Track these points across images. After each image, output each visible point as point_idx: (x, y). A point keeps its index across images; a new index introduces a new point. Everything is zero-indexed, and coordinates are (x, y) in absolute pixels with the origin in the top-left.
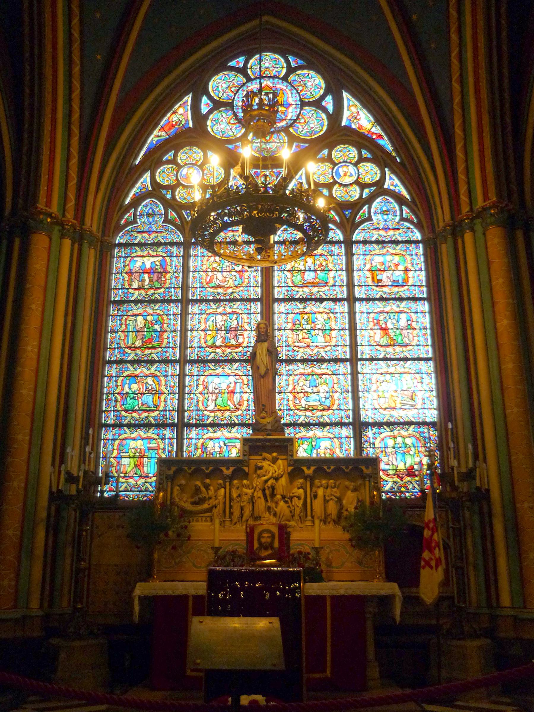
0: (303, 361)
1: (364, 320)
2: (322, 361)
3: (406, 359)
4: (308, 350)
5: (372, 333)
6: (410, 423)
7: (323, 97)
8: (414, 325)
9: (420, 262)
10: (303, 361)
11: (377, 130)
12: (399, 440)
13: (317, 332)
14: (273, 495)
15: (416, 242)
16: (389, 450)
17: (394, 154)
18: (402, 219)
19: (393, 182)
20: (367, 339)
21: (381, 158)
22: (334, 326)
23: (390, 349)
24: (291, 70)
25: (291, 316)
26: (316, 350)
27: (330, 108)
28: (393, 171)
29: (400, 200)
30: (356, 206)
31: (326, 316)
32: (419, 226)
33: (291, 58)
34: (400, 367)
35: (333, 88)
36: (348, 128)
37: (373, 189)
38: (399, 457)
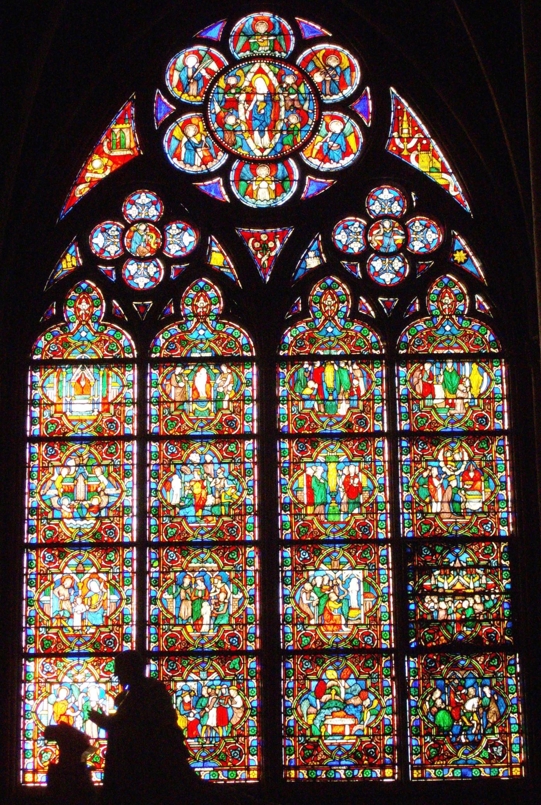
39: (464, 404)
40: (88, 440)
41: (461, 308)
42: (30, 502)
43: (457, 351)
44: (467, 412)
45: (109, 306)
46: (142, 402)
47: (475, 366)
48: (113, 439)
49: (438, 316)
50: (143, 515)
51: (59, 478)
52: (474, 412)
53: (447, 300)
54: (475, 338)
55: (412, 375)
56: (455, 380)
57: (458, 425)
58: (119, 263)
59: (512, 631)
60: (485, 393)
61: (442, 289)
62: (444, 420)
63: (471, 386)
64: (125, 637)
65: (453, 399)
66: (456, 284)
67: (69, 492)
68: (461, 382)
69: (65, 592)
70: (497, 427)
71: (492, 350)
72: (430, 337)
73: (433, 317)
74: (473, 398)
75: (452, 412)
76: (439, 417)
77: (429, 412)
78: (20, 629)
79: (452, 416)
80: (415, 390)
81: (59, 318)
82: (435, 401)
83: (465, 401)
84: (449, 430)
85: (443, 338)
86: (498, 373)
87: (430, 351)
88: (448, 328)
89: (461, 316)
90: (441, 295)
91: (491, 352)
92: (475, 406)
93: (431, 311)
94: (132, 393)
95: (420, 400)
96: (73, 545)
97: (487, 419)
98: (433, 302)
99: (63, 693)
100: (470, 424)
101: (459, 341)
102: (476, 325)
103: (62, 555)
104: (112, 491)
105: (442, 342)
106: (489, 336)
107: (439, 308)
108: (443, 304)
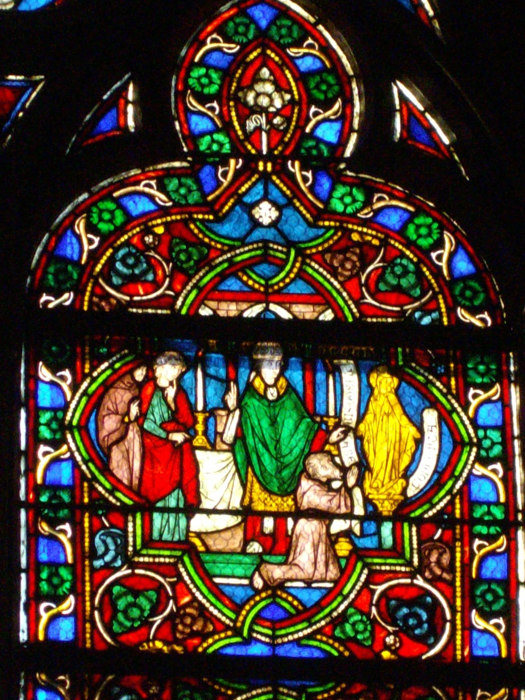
39: (332, 540)
41: (329, 133)
43: (305, 311)
44: (345, 574)
47: (384, 383)
49: (224, 160)
52: (375, 577)
53: (266, 94)
54: (389, 262)
55: (96, 403)
56: (292, 435)
57: (301, 630)
60: (427, 495)
61: (245, 48)
62: (237, 608)
63: (363, 465)
65: (279, 517)
66: (306, 31)
68: (318, 442)
70: (483, 647)
71: (462, 314)
72: (184, 248)
73: (200, 159)
74: (373, 516)
75: (278, 573)
76: (217, 591)
77: (170, 570)
79: (276, 588)
80: (105, 469)
82: (200, 523)
83: (338, 526)
84: (256, 650)
85: (243, 255)
86: (490, 415)
87: (183, 305)
88: (266, 213)
89: (326, 163)
90: (236, 75)
91: (458, 324)
92: (380, 551)
93: (193, 138)
95: (125, 511)
97: (434, 608)
98: (203, 99)
100: (355, 627)
101: (314, 269)
102: (391, 207)
105: (234, 270)
106: (450, 256)
107: (227, 128)
108: (246, 111)
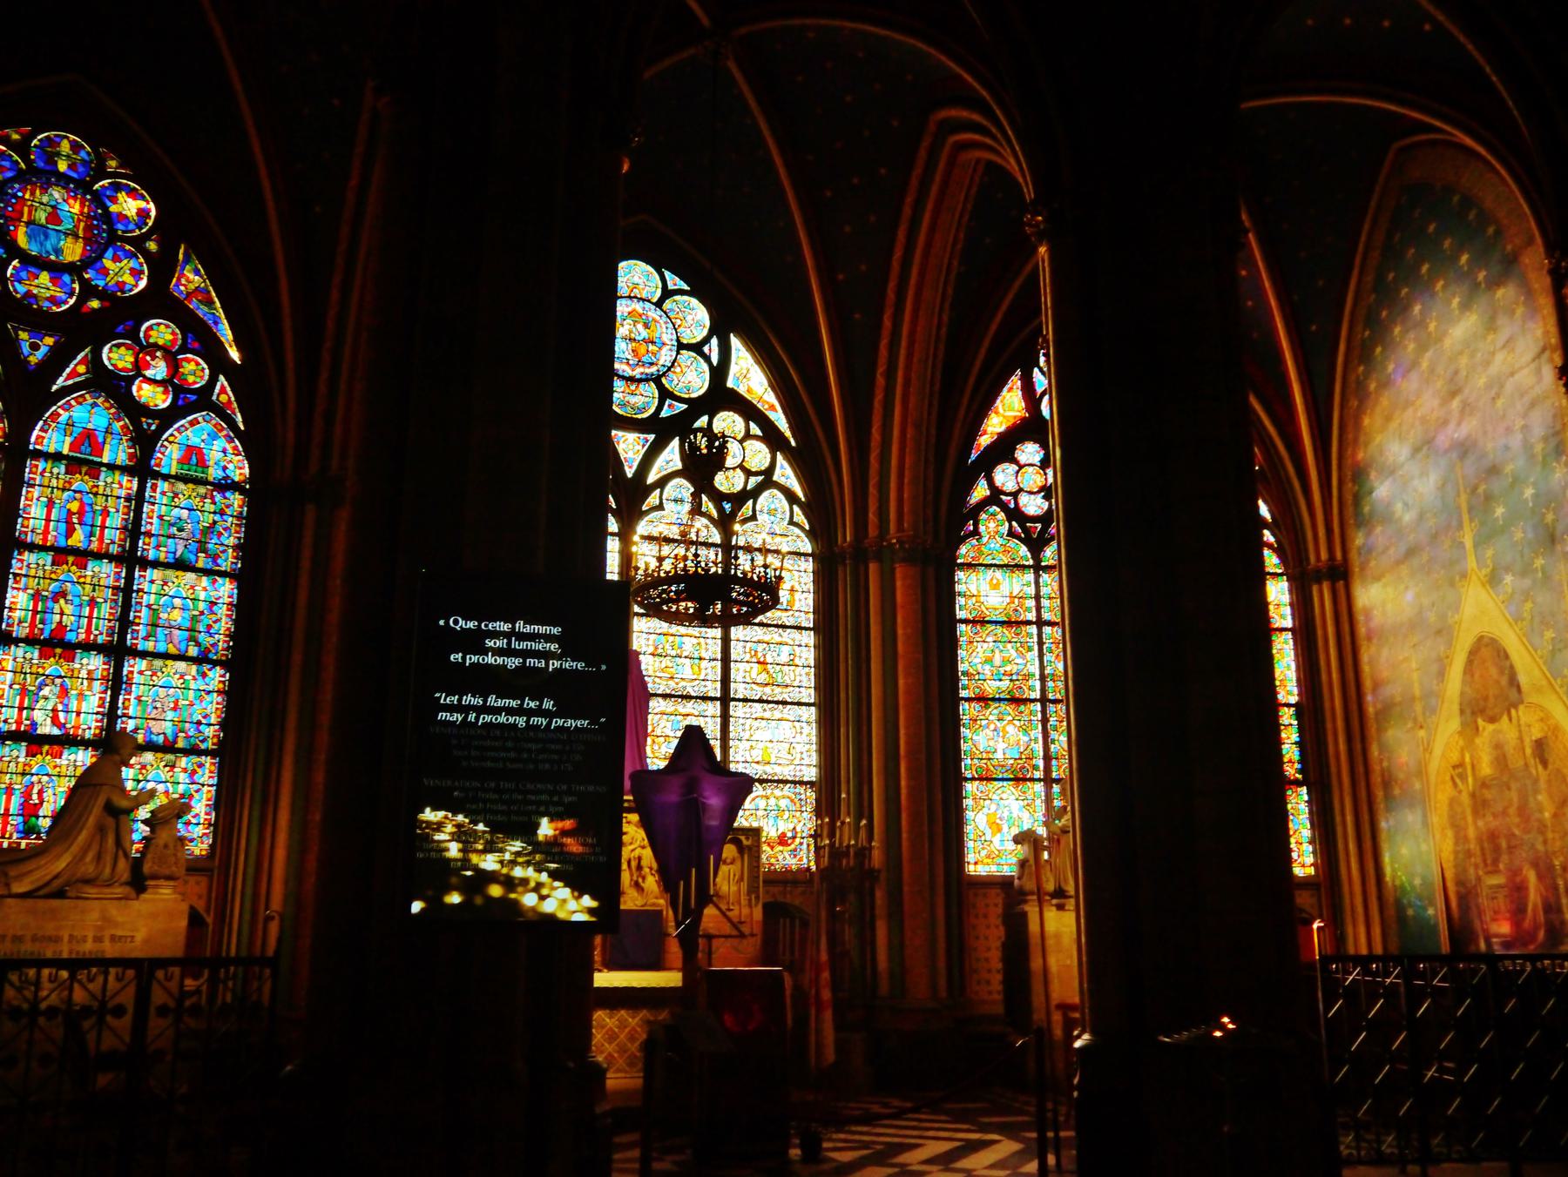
0: (665, 696)
1: (741, 650)
2: (688, 697)
3: (784, 703)
4: (672, 684)
5: (748, 666)
6: (785, 782)
7: (706, 340)
8: (797, 661)
9: (808, 579)
10: (665, 696)
11: (771, 398)
12: (772, 801)
13: (683, 660)
14: (639, 868)
15: (805, 555)
16: (760, 813)
17: (788, 434)
18: (792, 522)
19: (785, 473)
20: (742, 674)
21: (772, 437)
22: (704, 655)
23: (768, 690)
24: (667, 293)
25: (653, 637)
26: (683, 683)
27: (715, 360)
28: (786, 458)
29: (791, 497)
30: (740, 498)
31: (695, 641)
32: (812, 534)
33: (667, 274)
34: (779, 712)
35: (720, 329)
36: (733, 392)
37: (760, 478)
38: (771, 821)
40: (1002, 623)
42: (962, 667)
45: (1011, 526)
46: (1038, 597)
48: (1019, 623)
50: (1043, 678)
51: (982, 650)
58: (1015, 495)
59: (1300, 771)
64: (1035, 768)
67: (989, 660)
69: (991, 734)
78: (961, 760)
81: (976, 533)
94: (1032, 590)
96: (993, 699)
99: (993, 807)
103: (987, 706)
104: (1020, 661)
